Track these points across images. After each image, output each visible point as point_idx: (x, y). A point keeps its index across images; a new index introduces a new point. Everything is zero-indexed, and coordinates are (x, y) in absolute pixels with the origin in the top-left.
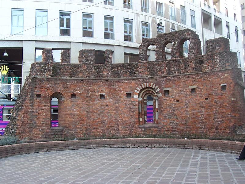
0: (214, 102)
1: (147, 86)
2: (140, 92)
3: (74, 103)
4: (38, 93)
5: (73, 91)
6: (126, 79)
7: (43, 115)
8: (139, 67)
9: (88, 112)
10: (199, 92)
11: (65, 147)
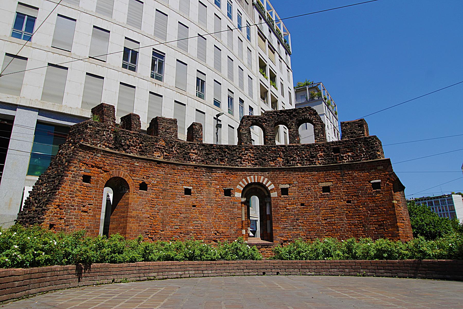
1: (254, 180)
3: (142, 199)
4: (86, 174)
5: (144, 178)
7: (89, 216)
9: (164, 216)
10: (336, 191)
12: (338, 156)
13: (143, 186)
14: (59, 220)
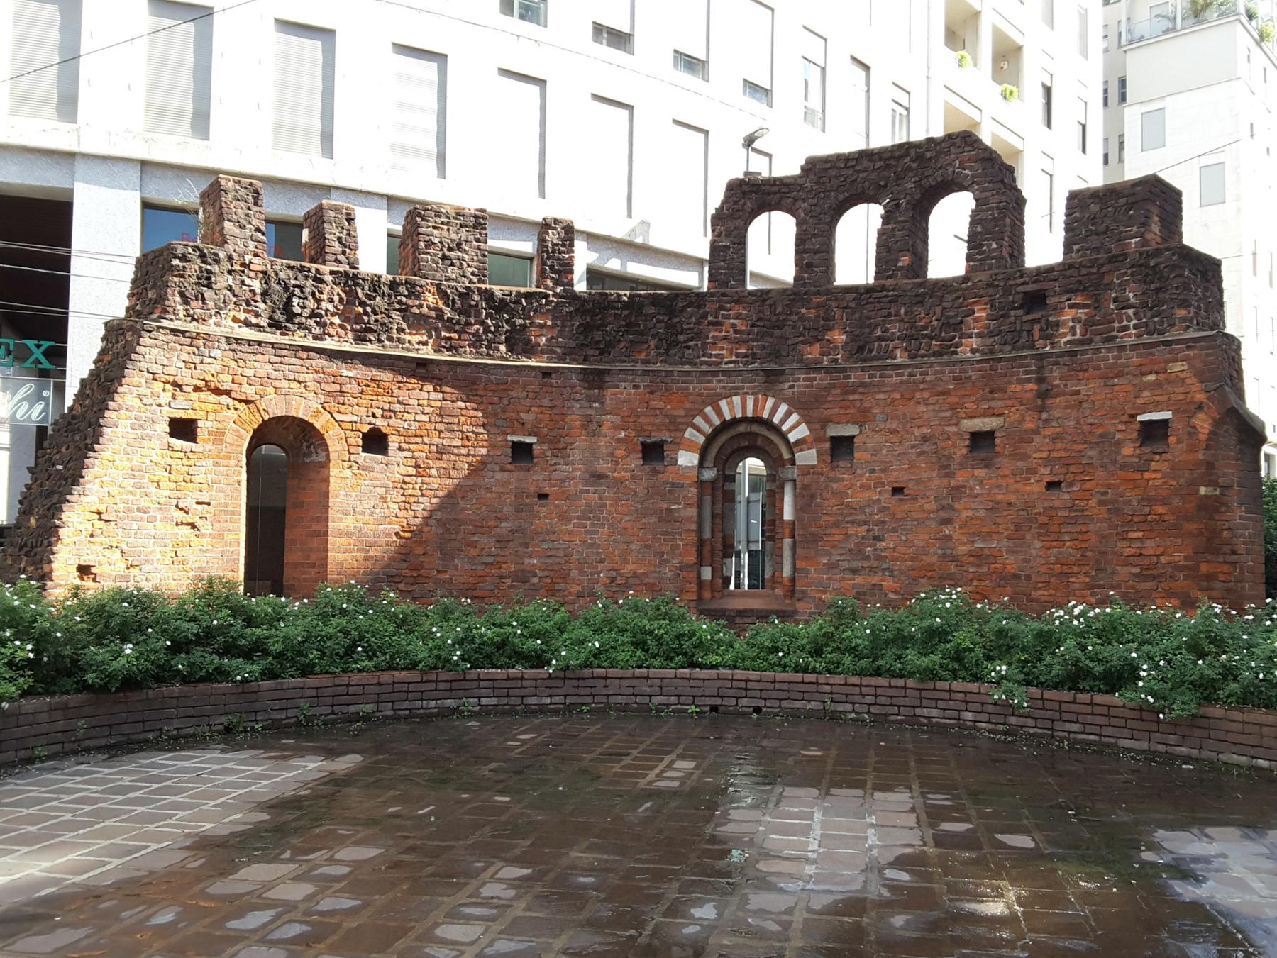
0: (1093, 503)
2: (710, 439)
5: (374, 415)
6: (645, 373)
8: (710, 318)
11: (332, 706)
12: (1038, 321)
13: (375, 441)
14: (107, 552)
